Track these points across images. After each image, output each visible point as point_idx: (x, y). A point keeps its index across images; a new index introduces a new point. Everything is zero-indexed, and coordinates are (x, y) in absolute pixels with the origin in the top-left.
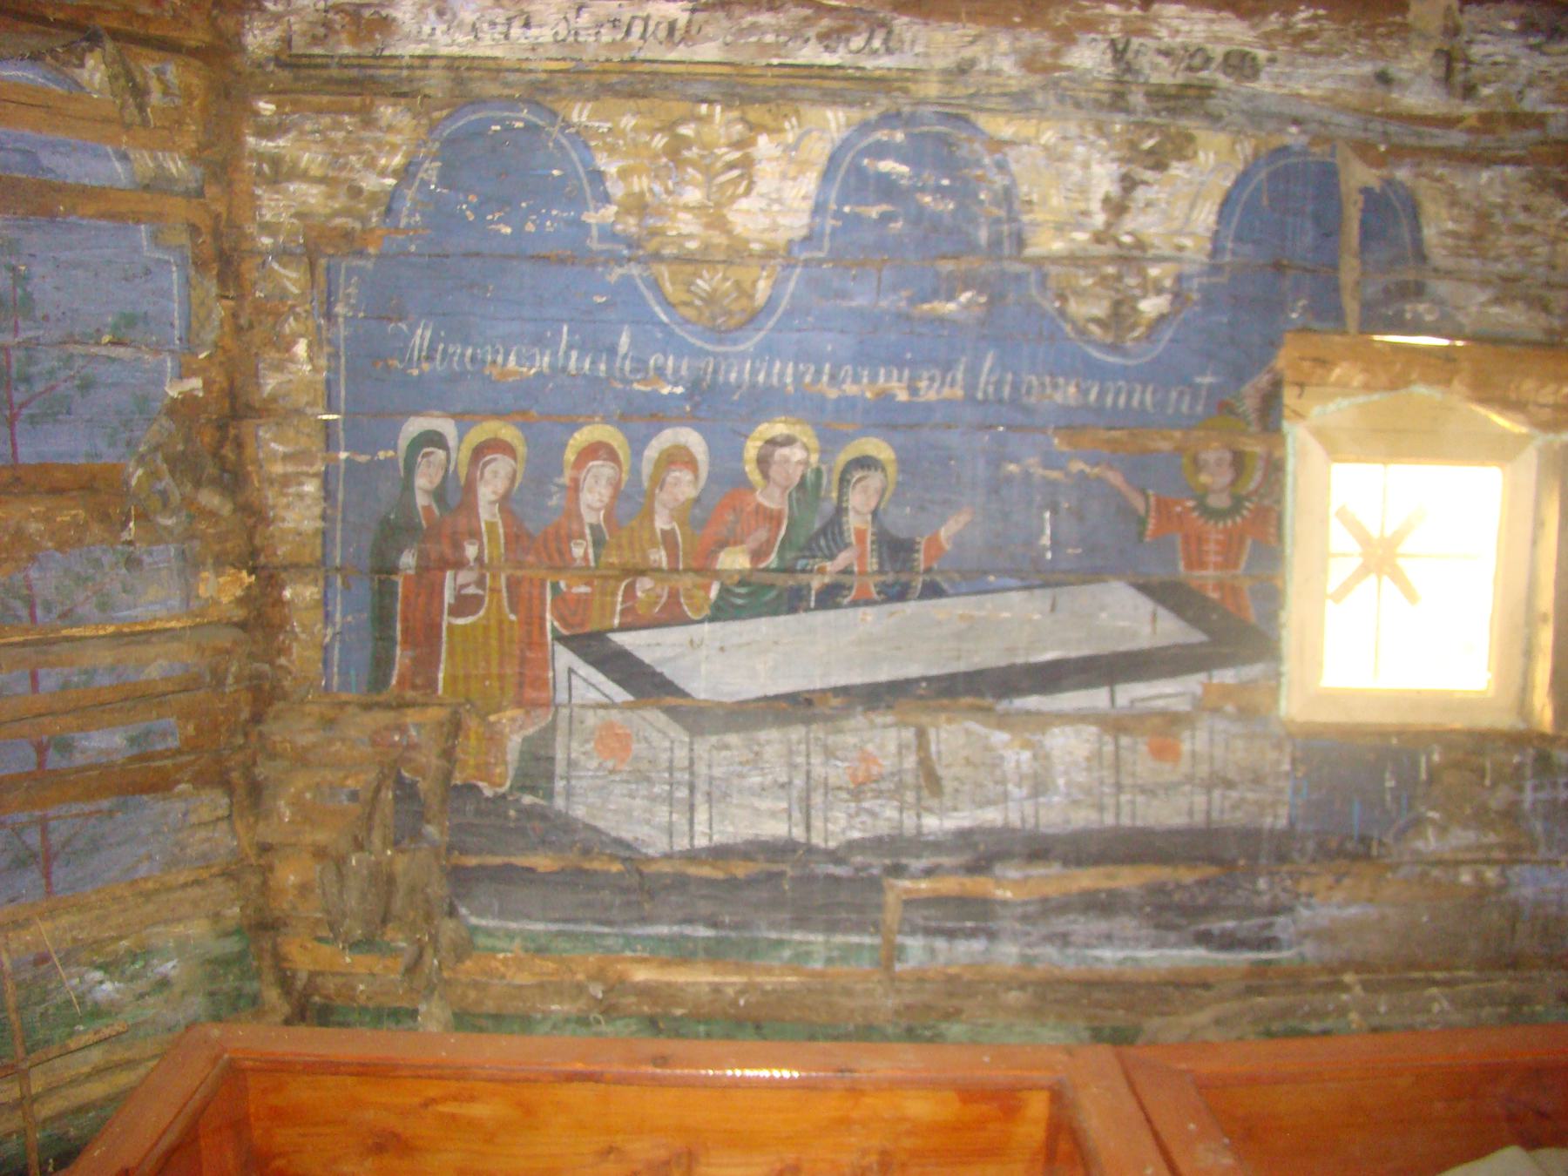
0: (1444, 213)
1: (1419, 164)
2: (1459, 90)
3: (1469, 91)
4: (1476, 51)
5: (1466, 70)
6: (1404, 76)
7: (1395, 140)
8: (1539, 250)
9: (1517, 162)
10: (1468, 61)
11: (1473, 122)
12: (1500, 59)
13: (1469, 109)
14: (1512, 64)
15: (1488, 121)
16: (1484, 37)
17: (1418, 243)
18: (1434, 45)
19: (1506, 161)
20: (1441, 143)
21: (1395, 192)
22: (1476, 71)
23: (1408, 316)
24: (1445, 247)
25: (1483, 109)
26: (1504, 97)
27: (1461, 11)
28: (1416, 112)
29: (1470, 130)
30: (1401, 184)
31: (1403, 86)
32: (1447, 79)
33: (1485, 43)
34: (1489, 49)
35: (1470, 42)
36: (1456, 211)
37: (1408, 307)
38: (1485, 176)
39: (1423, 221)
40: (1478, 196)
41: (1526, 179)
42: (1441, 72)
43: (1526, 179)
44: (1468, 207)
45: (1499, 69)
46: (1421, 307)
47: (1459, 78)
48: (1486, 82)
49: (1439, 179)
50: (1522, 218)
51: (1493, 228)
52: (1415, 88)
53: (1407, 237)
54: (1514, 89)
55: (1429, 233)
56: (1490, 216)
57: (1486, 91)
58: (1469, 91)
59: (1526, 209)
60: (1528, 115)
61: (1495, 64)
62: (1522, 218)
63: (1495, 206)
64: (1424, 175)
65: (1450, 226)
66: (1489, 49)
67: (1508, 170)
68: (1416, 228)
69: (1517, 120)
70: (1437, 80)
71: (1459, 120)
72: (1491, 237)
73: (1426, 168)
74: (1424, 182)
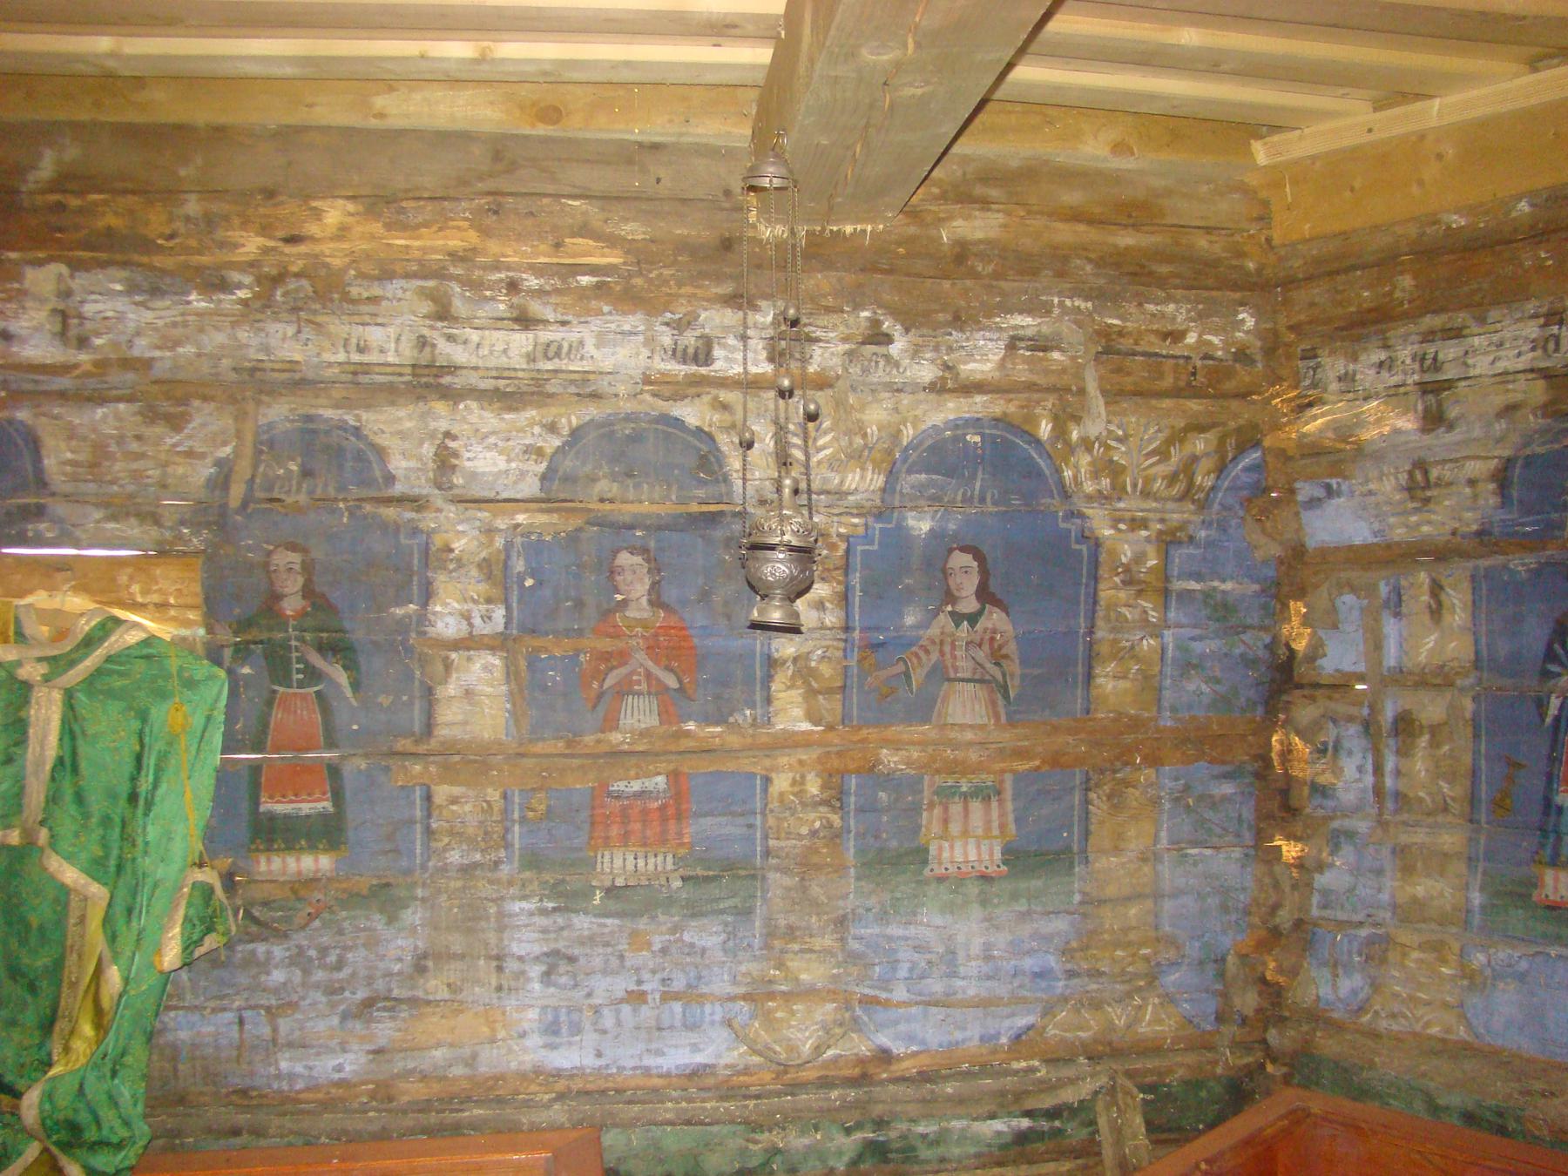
0: (63, 445)
1: (38, 406)
2: (74, 342)
3: (83, 342)
4: (89, 309)
5: (81, 324)
6: (24, 332)
7: (14, 386)
8: (150, 473)
9: (130, 399)
10: (81, 317)
11: (88, 367)
12: (110, 314)
13: (84, 357)
14: (121, 317)
15: (102, 365)
16: (94, 297)
17: (39, 471)
18: (50, 306)
19: (119, 399)
20: (54, 387)
21: (17, 430)
22: (89, 325)
23: (30, 534)
24: (65, 474)
25: (98, 357)
26: (115, 345)
27: (72, 277)
28: (36, 362)
29: (87, 375)
30: (21, 422)
31: (23, 341)
32: (63, 334)
33: (96, 302)
34: (100, 307)
35: (82, 302)
36: (74, 443)
37: (30, 527)
38: (100, 412)
39: (44, 452)
40: (94, 430)
41: (140, 413)
42: (58, 327)
43: (140, 413)
44: (85, 439)
45: (107, 323)
46: (42, 526)
47: (73, 332)
48: (98, 334)
49: (56, 418)
50: (134, 446)
51: (110, 457)
52: (33, 342)
53: (30, 468)
54: (124, 338)
55: (49, 462)
56: (108, 446)
57: (98, 342)
58: (83, 342)
59: (138, 438)
60: (138, 359)
61: (106, 318)
62: (134, 446)
63: (112, 436)
64: (45, 415)
65: (69, 455)
66: (100, 307)
67: (122, 406)
68: (37, 458)
69: (127, 364)
70: (54, 334)
71: (76, 366)
72: (108, 464)
73: (45, 409)
74: (44, 420)
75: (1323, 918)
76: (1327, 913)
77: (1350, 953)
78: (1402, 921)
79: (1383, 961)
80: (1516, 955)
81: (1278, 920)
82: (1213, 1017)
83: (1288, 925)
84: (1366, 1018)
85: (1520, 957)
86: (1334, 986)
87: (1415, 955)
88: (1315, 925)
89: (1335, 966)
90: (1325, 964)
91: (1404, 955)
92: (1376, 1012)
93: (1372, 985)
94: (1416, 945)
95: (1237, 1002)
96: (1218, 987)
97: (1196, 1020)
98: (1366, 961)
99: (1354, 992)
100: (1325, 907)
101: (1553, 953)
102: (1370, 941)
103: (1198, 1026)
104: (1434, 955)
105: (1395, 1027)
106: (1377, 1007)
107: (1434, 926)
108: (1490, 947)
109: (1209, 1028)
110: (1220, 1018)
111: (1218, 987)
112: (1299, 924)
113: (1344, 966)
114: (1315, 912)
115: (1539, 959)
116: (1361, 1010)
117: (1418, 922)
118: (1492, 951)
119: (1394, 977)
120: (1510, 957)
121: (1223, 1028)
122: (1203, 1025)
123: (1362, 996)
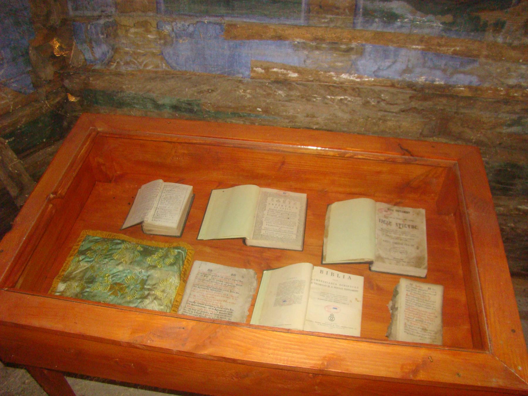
75: (76, 16)
76: (78, 13)
77: (97, 34)
78: (122, 12)
79: (116, 35)
80: (187, 24)
81: (52, 22)
82: (32, 86)
83: (59, 23)
84: (113, 66)
85: (189, 26)
86: (93, 53)
87: (133, 30)
88: (74, 21)
89: (91, 42)
90: (85, 42)
91: (127, 31)
92: (118, 62)
93: (113, 49)
94: (132, 25)
95: (43, 75)
96: (30, 69)
97: (23, 91)
98: (107, 37)
99: (104, 54)
100: (76, 9)
101: (206, 21)
102: (106, 26)
103: (24, 93)
104: (143, 29)
105: (129, 69)
106: (118, 60)
107: (140, 13)
108: (172, 22)
109: (32, 91)
110: (36, 86)
111: (30, 69)
112: (64, 22)
113: (96, 42)
114: (71, 13)
115: (198, 25)
116: (109, 63)
117: (131, 12)
118: (174, 24)
119: (124, 43)
120: (183, 25)
121: (40, 90)
122: (27, 91)
123: (108, 56)
